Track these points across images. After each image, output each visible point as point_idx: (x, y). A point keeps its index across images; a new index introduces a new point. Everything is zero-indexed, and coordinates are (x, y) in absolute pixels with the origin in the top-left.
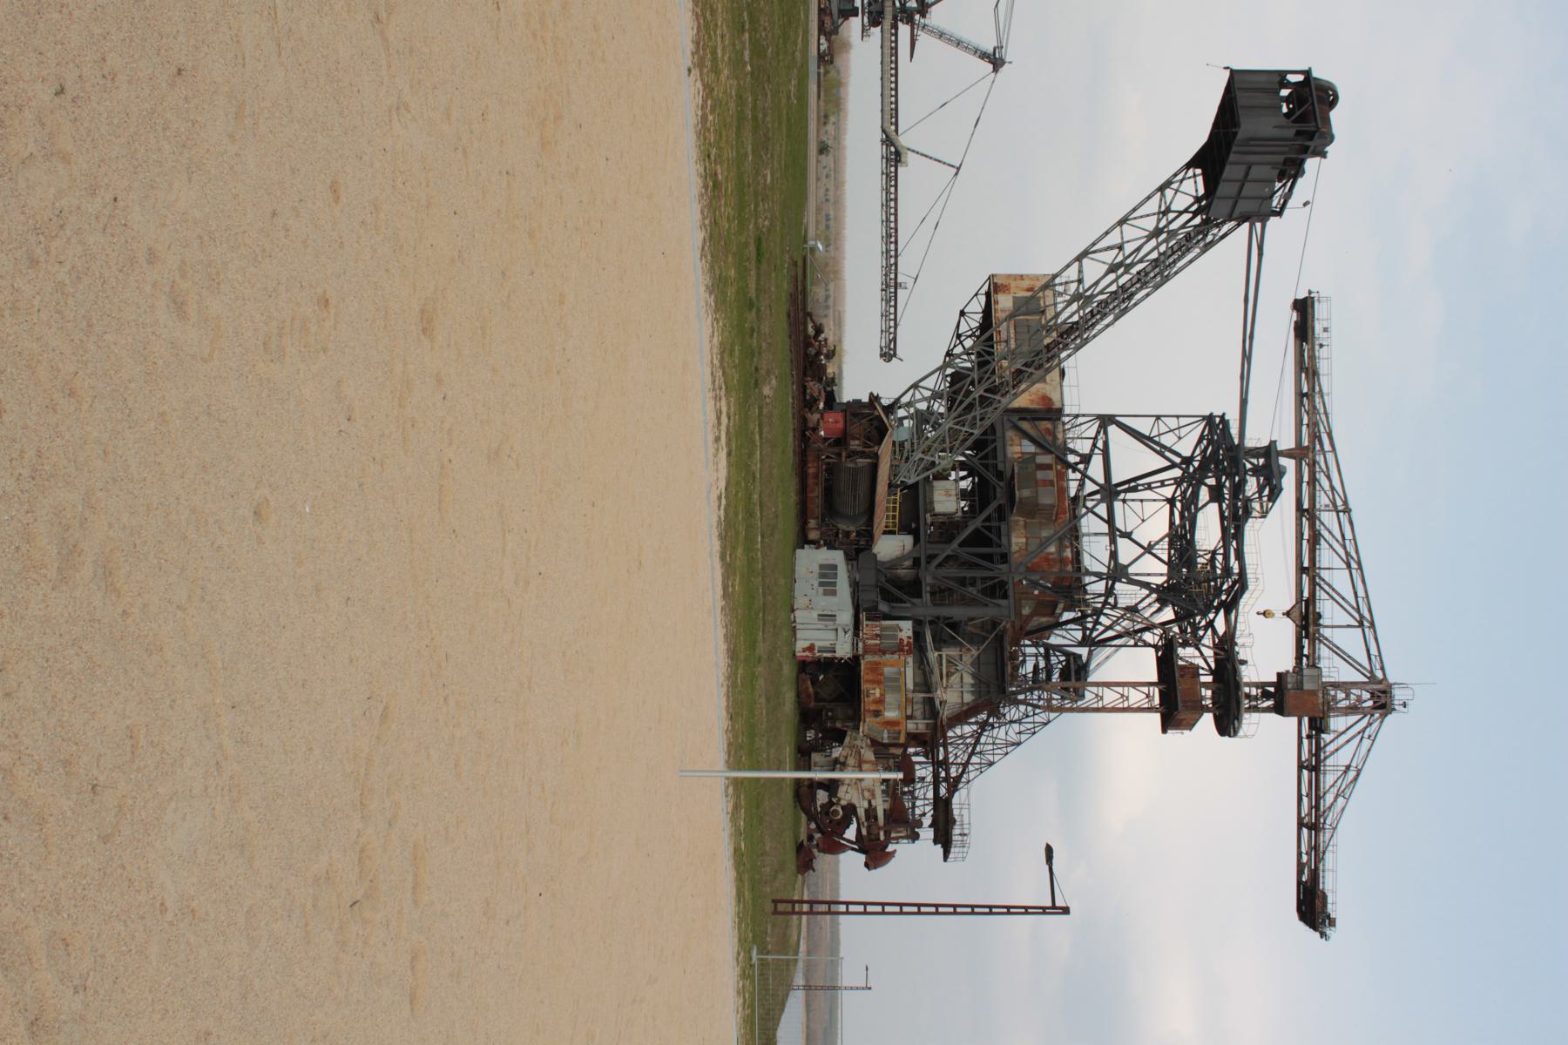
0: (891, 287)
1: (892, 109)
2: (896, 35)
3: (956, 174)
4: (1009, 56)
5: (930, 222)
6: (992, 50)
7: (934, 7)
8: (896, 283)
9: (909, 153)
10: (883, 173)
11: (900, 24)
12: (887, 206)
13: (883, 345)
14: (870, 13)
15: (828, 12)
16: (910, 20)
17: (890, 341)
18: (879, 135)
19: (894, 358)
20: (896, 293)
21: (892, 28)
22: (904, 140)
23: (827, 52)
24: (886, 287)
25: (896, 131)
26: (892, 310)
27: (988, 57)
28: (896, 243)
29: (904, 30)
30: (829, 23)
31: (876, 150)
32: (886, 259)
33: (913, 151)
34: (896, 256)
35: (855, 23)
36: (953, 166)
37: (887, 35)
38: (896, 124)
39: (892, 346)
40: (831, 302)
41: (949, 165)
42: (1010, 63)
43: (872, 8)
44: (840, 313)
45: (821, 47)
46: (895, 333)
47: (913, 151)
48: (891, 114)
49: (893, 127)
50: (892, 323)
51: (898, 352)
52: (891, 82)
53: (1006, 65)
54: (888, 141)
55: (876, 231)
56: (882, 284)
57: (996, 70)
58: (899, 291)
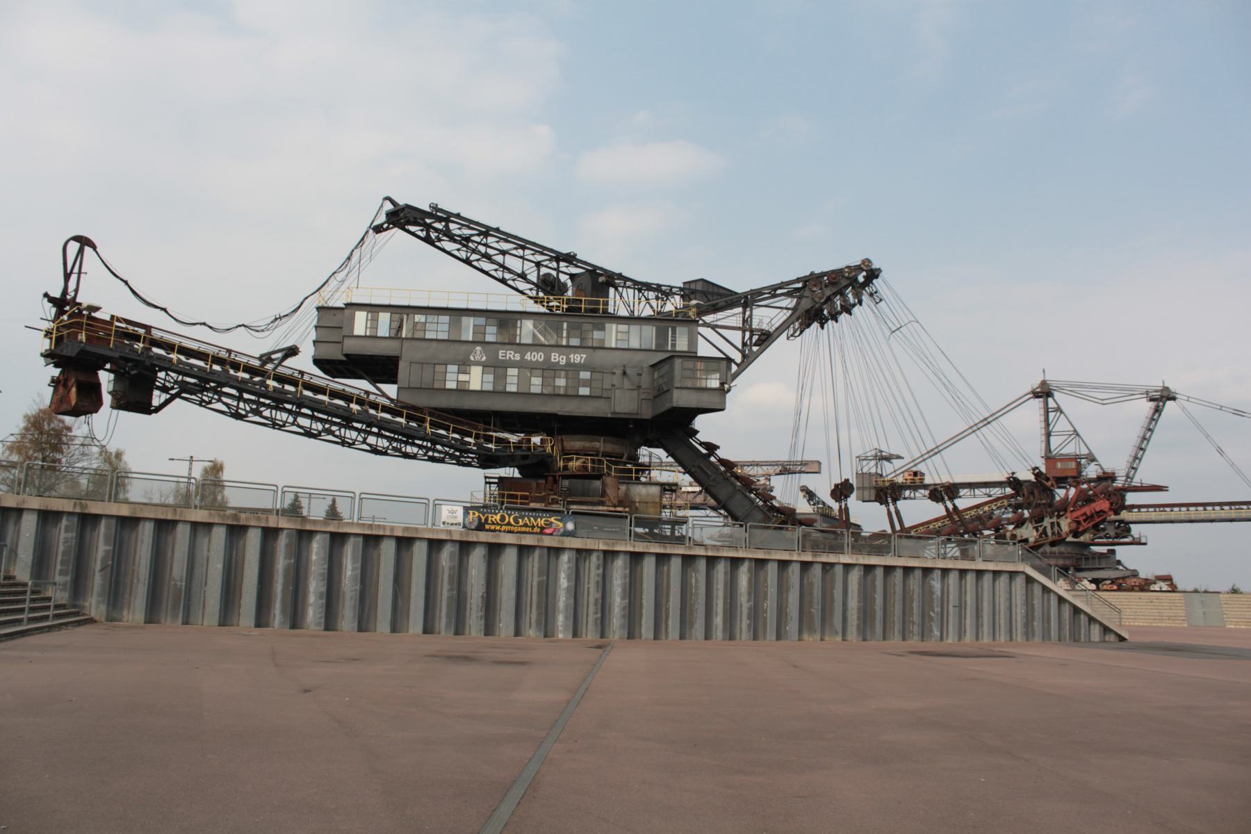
4: (1155, 383)
6: (1152, 404)
7: (1104, 466)
14: (1117, 536)
15: (1121, 581)
21: (1132, 512)
23: (1169, 583)
27: (1158, 406)
29: (1131, 499)
30: (1135, 580)
35: (1124, 554)
42: (1164, 383)
43: (1112, 533)
45: (1163, 589)
53: (1166, 385)
57: (1174, 399)
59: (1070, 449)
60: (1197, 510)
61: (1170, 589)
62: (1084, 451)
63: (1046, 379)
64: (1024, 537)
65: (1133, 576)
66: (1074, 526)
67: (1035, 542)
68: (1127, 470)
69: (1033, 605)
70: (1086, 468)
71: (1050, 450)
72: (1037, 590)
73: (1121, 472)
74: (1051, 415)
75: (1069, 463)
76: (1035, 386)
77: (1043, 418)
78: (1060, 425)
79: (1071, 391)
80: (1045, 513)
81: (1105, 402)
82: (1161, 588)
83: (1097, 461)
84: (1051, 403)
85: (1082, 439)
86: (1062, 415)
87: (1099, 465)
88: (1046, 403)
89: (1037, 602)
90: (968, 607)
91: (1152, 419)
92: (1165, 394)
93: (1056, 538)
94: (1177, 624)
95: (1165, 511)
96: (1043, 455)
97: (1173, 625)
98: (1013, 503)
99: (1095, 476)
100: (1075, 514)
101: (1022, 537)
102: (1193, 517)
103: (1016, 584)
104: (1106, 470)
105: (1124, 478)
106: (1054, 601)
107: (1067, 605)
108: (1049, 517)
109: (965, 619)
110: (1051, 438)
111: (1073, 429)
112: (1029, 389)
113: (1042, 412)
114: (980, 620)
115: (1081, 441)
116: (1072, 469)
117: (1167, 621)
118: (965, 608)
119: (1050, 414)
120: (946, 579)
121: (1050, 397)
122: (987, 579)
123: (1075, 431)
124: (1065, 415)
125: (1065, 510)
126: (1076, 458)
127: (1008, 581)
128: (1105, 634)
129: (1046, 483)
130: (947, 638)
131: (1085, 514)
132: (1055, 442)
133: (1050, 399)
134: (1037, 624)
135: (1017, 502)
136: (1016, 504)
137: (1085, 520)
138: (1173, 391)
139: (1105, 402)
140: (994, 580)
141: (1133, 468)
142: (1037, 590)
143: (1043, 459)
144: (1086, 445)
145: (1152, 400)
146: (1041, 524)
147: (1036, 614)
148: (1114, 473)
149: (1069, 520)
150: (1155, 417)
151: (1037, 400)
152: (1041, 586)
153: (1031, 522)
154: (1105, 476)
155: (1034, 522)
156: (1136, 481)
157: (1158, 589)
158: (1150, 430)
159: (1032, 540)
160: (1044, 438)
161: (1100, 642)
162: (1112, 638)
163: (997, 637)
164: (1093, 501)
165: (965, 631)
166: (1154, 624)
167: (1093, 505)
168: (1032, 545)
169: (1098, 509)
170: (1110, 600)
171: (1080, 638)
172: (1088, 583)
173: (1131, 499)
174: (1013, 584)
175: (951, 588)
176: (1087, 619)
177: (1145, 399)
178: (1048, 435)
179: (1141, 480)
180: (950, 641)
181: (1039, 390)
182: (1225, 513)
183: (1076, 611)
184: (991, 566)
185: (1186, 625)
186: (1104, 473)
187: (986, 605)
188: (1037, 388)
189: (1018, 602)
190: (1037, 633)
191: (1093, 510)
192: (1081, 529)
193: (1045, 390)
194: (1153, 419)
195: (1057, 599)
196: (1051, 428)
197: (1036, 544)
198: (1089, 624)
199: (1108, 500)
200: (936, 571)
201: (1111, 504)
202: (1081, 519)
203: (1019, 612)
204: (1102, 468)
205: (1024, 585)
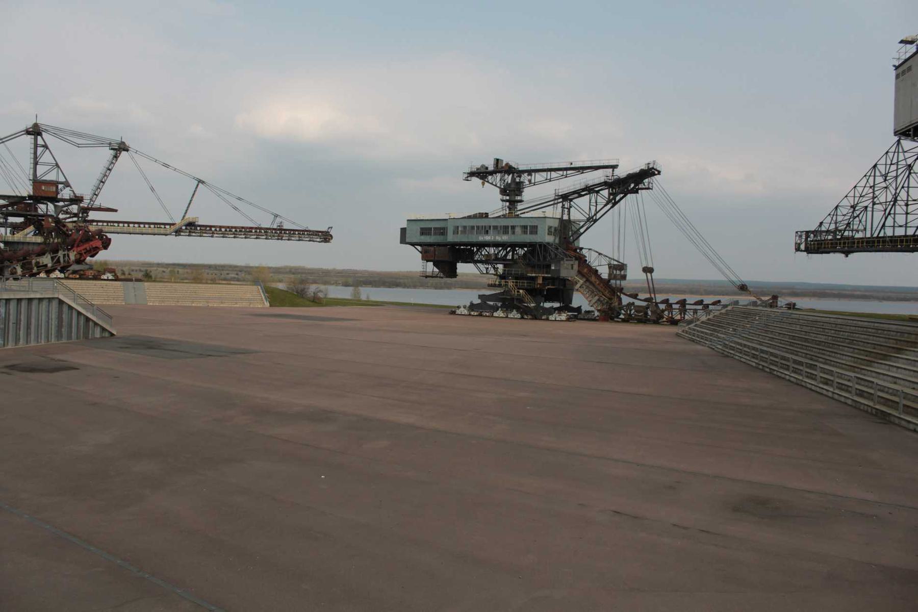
0: (280, 233)
1: (155, 227)
2: (98, 221)
3: (203, 182)
5: (238, 204)
6: (112, 152)
8: (279, 230)
9: (187, 217)
10: (189, 236)
11: (89, 218)
12: (225, 234)
13: (318, 240)
15: (82, 272)
16: (85, 210)
17: (316, 235)
18: (172, 238)
19: (331, 233)
20: (284, 230)
21: (92, 225)
22: (178, 220)
23: (113, 274)
24: (280, 238)
25: (173, 224)
26: (297, 233)
27: (116, 154)
28: (252, 228)
30: (91, 272)
31: (184, 239)
32: (263, 235)
33: (186, 213)
34: (261, 229)
36: (198, 185)
37: (112, 229)
38: (165, 224)
39: (320, 234)
40: (142, 269)
41: (196, 188)
42: (122, 139)
44: (142, 264)
45: (109, 278)
46: (313, 231)
47: (186, 213)
48: (158, 228)
49: (168, 227)
50: (306, 233)
51: (324, 230)
52: (144, 227)
53: (123, 141)
54: (178, 232)
55: (241, 243)
56: (278, 239)
57: (127, 150)
58: (284, 228)
59: (52, 177)
60: (134, 227)
61: (113, 278)
62: (62, 179)
63: (38, 122)
64: (45, 263)
65: (90, 269)
66: (78, 256)
67: (52, 267)
68: (91, 195)
69: (62, 318)
70: (61, 191)
71: (36, 175)
72: (65, 309)
73: (87, 196)
74: (40, 150)
75: (51, 187)
76: (28, 127)
77: (32, 151)
78: (46, 158)
79: (54, 133)
80: (59, 247)
81: (80, 146)
82: (108, 277)
83: (71, 188)
84: (40, 141)
85: (60, 169)
86: (48, 150)
87: (73, 191)
88: (36, 140)
89: (65, 316)
90: (22, 323)
91: (112, 163)
92: (122, 146)
93: (66, 264)
94: (119, 303)
95: (115, 226)
96: (31, 179)
97: (116, 303)
98: (5, 212)
99: (68, 198)
100: (79, 249)
101: (43, 263)
102: (131, 231)
103: (52, 305)
104: (77, 195)
105: (89, 201)
106: (75, 315)
107: (82, 317)
108: (62, 250)
109: (20, 331)
110: (38, 166)
111: (55, 162)
112: (23, 128)
113: (33, 146)
114: (29, 330)
115: (59, 170)
116: (53, 192)
117: (112, 301)
118: (20, 324)
119: (38, 148)
120: (8, 305)
121: (39, 135)
122: (35, 303)
123: (57, 165)
124: (50, 151)
125: (72, 247)
126: (55, 184)
127: (47, 304)
128: (103, 332)
129: (62, 228)
130: (8, 344)
131: (86, 249)
132: (41, 170)
133: (39, 137)
134: (64, 330)
135: (8, 212)
136: (6, 213)
137: (85, 253)
138: (127, 145)
139: (80, 146)
140: (39, 304)
141: (95, 194)
142: (65, 309)
143: (31, 182)
144: (63, 174)
145: (112, 149)
146: (56, 255)
147: (64, 324)
148: (82, 197)
149: (75, 253)
150: (114, 161)
151: (29, 136)
152: (67, 306)
153: (50, 253)
154: (77, 198)
155: (51, 254)
156: (97, 203)
157: (106, 278)
158: (110, 170)
159: (50, 265)
160: (32, 166)
161: (100, 338)
162: (107, 335)
163: (40, 340)
164: (92, 241)
165: (19, 339)
166: (104, 303)
167: (91, 243)
168: (50, 269)
169: (94, 246)
170: (87, 298)
171: (89, 336)
172: (59, 273)
173: (92, 215)
174: (50, 305)
175: (11, 311)
176: (93, 325)
177: (108, 148)
178: (36, 163)
179: (100, 204)
180: (10, 347)
181: (31, 130)
182: (151, 230)
183: (88, 319)
184: (38, 296)
185: (124, 304)
186: (76, 196)
187: (33, 321)
188: (30, 128)
189: (53, 317)
190: (64, 336)
191: (91, 247)
192: (82, 259)
193: (36, 131)
194: (112, 163)
195: (76, 313)
196: (38, 160)
197: (52, 268)
198: (94, 327)
199: (100, 240)
200: (2, 301)
201: (103, 243)
202: (83, 252)
203: (54, 323)
204: (74, 193)
205: (57, 306)
